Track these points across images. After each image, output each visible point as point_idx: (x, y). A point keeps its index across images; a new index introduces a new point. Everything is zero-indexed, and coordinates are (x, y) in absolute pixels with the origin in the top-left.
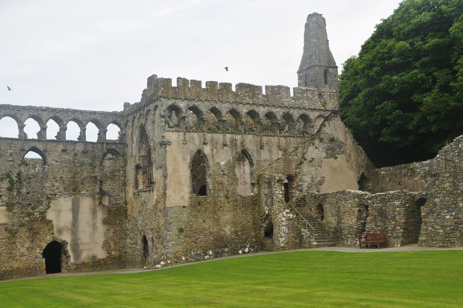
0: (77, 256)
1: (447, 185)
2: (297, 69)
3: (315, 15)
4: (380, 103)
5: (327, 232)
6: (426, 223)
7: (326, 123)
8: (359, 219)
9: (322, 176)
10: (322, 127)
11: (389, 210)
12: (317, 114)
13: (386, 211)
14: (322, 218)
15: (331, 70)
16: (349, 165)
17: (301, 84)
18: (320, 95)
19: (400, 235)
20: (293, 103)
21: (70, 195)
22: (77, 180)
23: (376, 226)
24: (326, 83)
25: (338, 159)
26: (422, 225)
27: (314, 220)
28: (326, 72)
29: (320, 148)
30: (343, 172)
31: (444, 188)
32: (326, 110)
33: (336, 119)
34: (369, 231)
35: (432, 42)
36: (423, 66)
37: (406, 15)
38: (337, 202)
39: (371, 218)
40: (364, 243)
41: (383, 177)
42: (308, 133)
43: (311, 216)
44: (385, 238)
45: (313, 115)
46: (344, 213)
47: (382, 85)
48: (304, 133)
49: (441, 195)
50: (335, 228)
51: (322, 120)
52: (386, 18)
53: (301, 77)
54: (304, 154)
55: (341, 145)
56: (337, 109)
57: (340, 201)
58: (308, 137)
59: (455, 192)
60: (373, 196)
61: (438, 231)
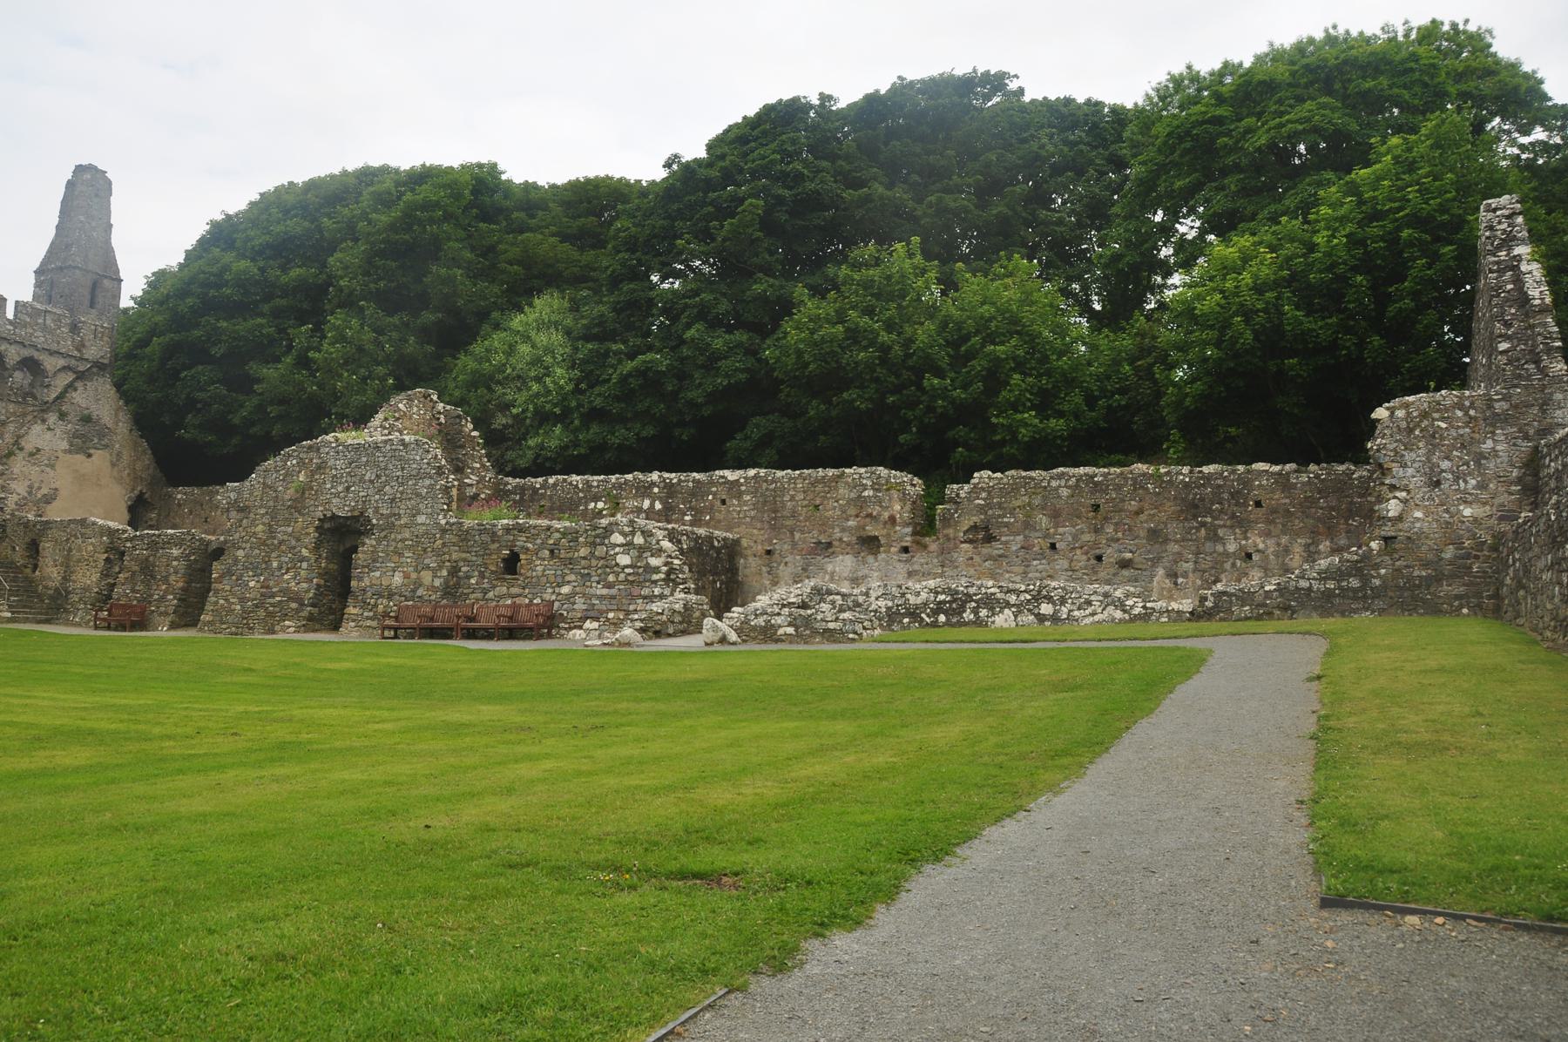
1: (260, 528)
2: (36, 265)
3: (91, 168)
4: (189, 368)
5: (40, 596)
6: (217, 591)
7: (79, 384)
8: (105, 574)
9: (53, 486)
10: (69, 390)
12: (61, 362)
14: (35, 567)
15: (106, 282)
16: (115, 474)
17: (39, 296)
18: (74, 328)
19: (171, 610)
20: (10, 330)
23: (133, 591)
24: (92, 305)
25: (94, 458)
26: (211, 594)
27: (18, 570)
28: (95, 287)
29: (58, 432)
30: (100, 485)
31: (254, 533)
32: (81, 359)
33: (101, 380)
34: (118, 599)
35: (295, 272)
36: (277, 314)
37: (265, 217)
38: (68, 539)
39: (127, 575)
40: (104, 620)
41: (179, 505)
42: (35, 398)
43: (12, 562)
44: (143, 613)
45: (50, 363)
46: (79, 561)
47: (197, 333)
48: (27, 395)
49: (249, 545)
50: (57, 589)
51: (70, 377)
52: (231, 213)
53: (42, 282)
54: (19, 437)
55: (103, 432)
56: (106, 361)
57: (73, 539)
58: (33, 405)
59: (269, 542)
60: (136, 536)
61: (233, 607)
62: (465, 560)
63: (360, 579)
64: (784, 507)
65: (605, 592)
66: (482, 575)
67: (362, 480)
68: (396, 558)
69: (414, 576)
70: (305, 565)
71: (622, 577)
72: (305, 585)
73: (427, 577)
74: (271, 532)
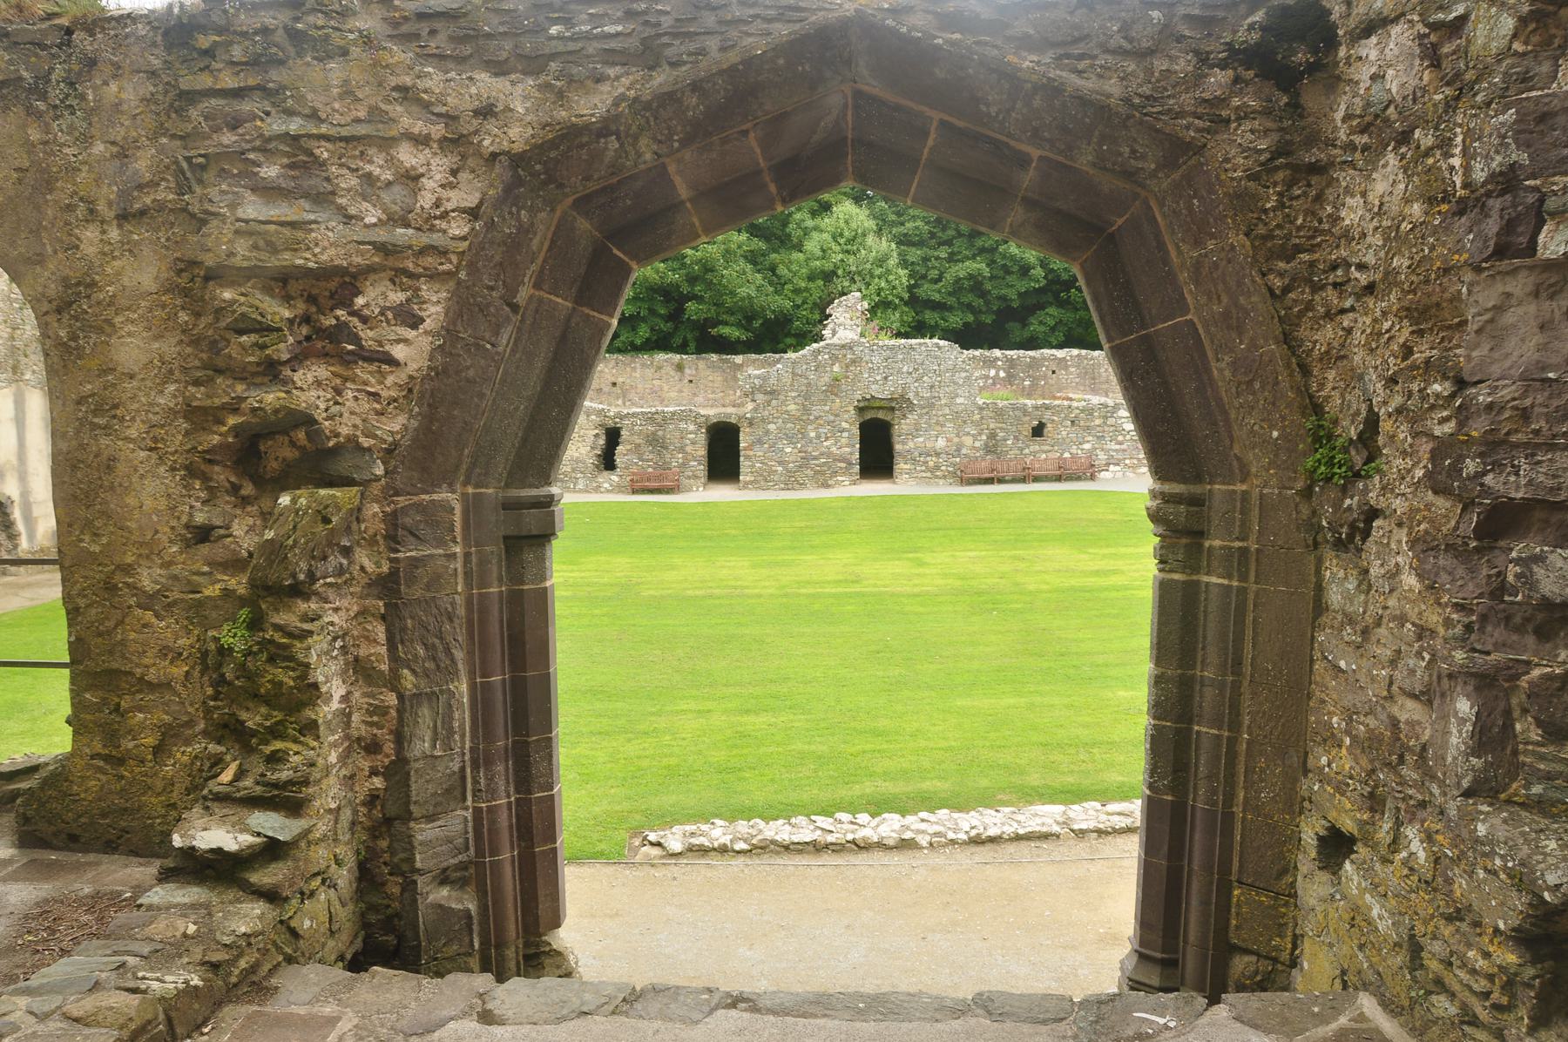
0: (31, 537)
1: (792, 407)
11: (670, 433)
13: (664, 438)
21: (10, 382)
22: (17, 343)
62: (1001, 429)
63: (904, 443)
64: (1100, 376)
65: (1118, 447)
66: (1016, 438)
67: (900, 371)
69: (956, 440)
70: (845, 434)
71: (1128, 437)
72: (847, 449)
73: (968, 441)
74: (806, 410)
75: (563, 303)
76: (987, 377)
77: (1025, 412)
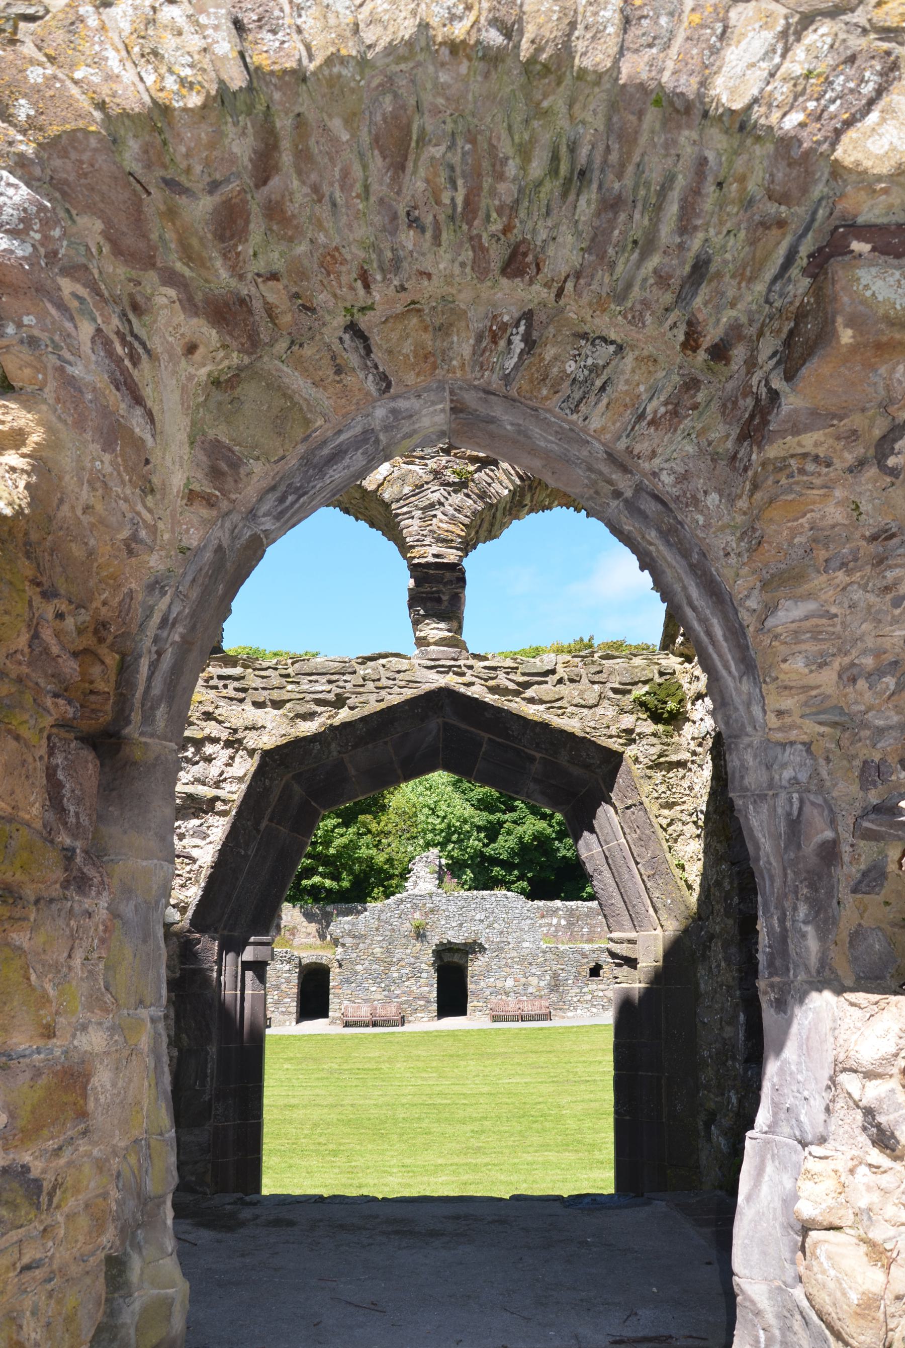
1: (378, 950)
63: (477, 983)
67: (473, 919)
68: (507, 969)
69: (523, 980)
72: (427, 989)
73: (534, 981)
74: (389, 952)
75: (283, 830)
76: (550, 925)
77: (584, 955)
